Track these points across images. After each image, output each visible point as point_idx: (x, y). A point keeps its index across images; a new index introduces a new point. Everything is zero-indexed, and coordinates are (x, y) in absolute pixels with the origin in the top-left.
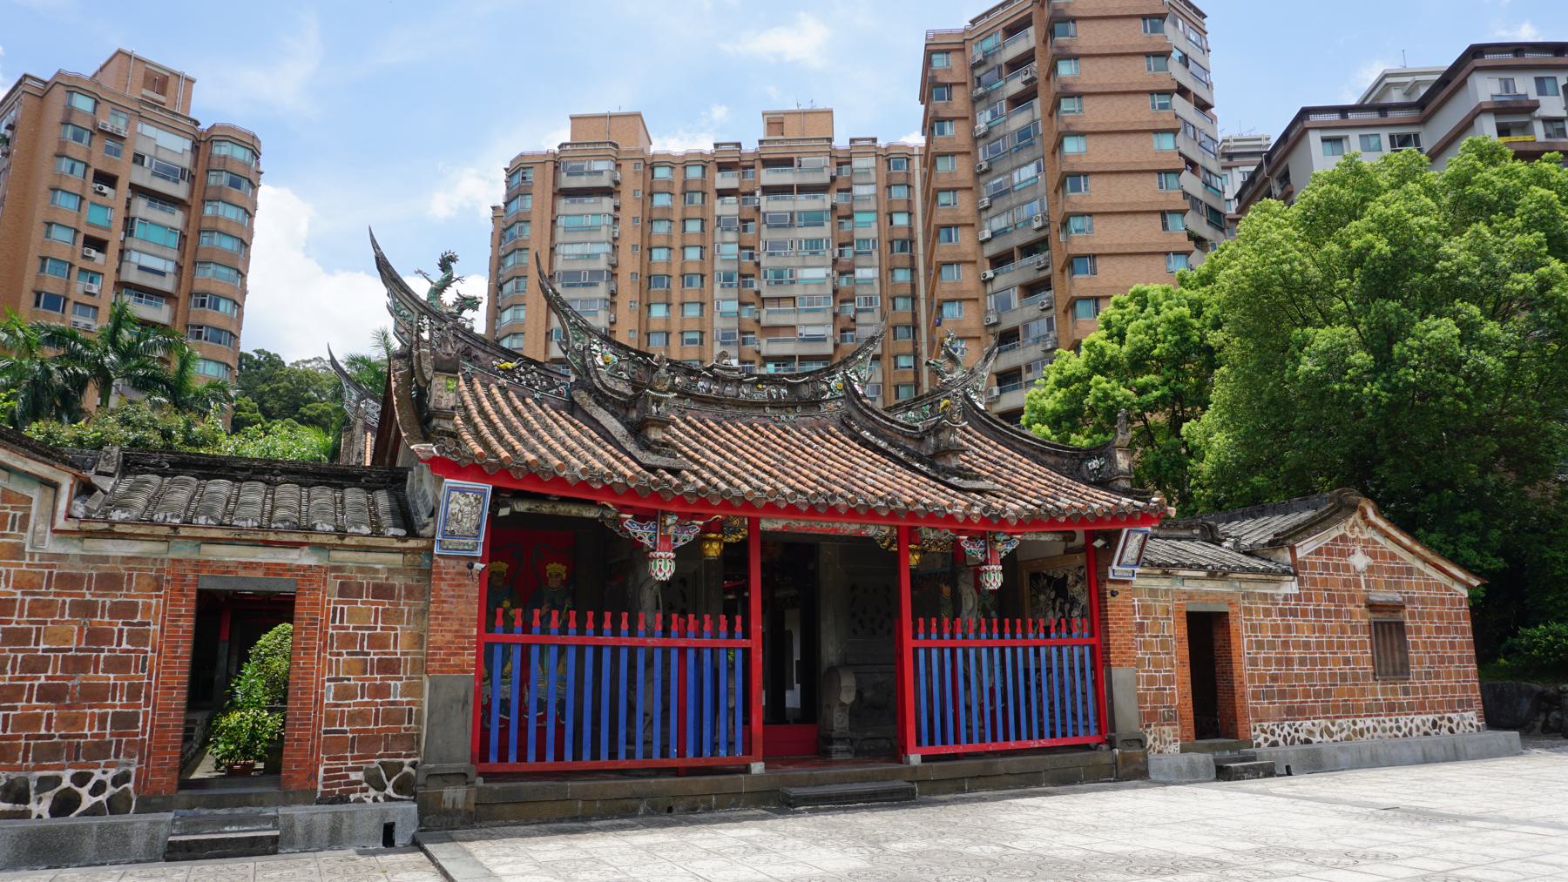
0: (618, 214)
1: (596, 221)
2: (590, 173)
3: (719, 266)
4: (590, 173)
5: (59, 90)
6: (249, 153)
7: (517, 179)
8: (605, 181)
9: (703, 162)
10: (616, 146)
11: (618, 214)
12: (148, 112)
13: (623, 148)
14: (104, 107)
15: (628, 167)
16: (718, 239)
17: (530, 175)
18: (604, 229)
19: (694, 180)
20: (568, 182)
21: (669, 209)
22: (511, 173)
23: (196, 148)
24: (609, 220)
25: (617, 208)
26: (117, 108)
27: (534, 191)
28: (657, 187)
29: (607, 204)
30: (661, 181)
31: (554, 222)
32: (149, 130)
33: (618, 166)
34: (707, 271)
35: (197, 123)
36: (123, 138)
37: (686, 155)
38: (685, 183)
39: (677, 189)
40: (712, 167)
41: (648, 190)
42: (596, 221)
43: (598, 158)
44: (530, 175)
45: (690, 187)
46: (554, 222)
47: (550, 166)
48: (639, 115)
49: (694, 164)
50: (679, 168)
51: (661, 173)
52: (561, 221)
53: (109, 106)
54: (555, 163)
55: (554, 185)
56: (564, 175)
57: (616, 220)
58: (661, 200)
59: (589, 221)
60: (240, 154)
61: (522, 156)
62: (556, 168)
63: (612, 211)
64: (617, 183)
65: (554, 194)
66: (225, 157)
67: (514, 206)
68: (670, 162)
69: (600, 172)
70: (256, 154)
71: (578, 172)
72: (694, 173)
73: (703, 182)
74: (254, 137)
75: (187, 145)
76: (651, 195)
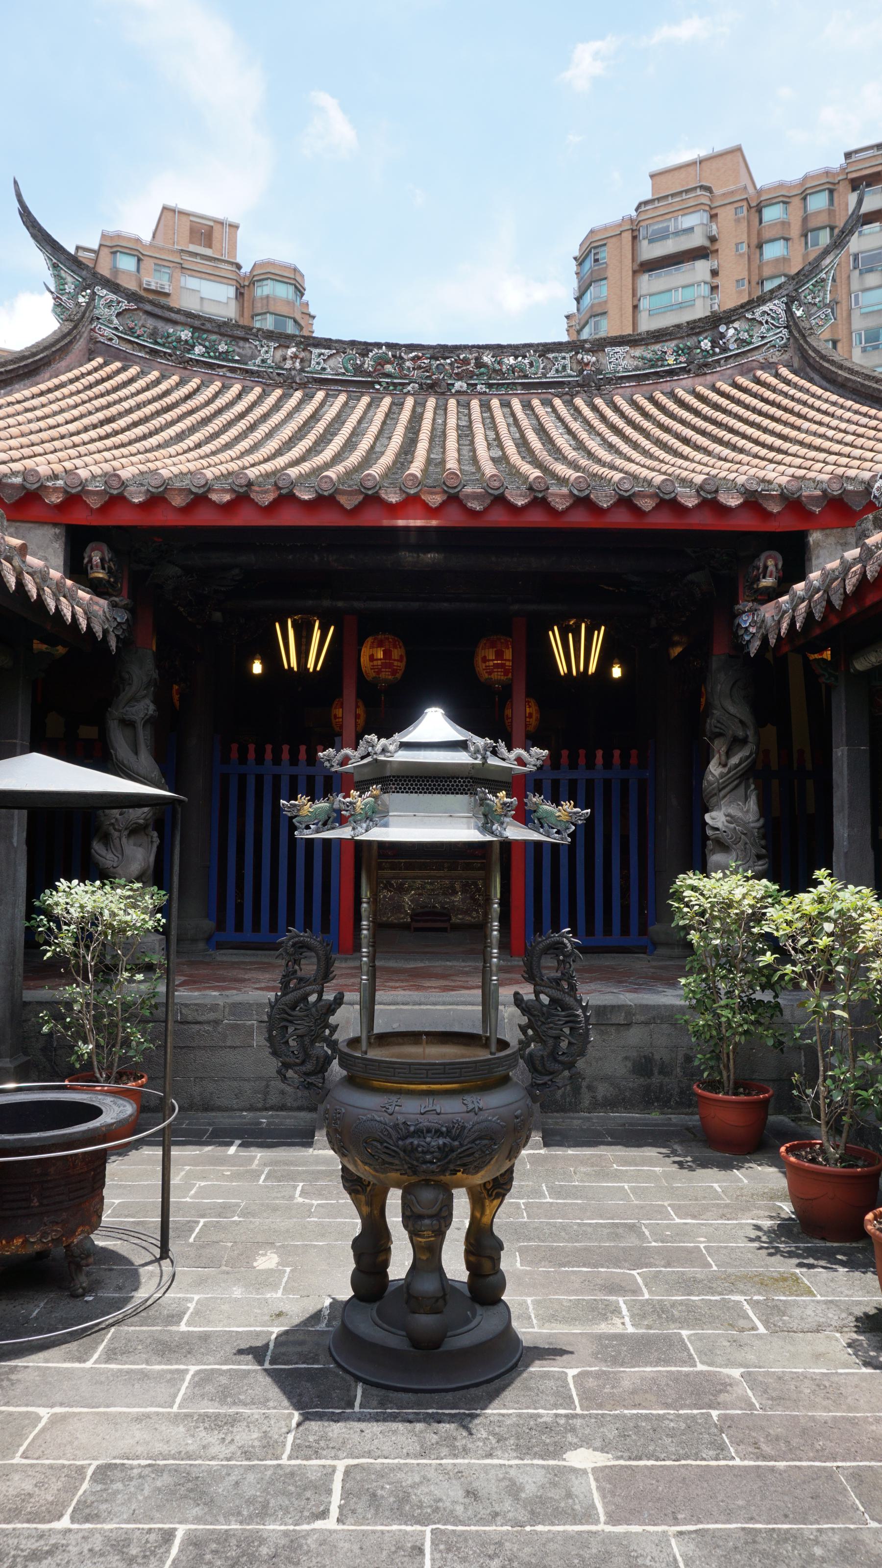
0: (716, 281)
1: (689, 294)
2: (677, 233)
3: (858, 323)
4: (677, 233)
5: (105, 252)
6: (291, 289)
7: (588, 265)
8: (697, 240)
9: (830, 185)
10: (708, 189)
11: (716, 281)
12: (190, 262)
13: (717, 191)
14: (148, 264)
15: (726, 215)
16: (855, 285)
17: (603, 255)
18: (699, 303)
19: (818, 213)
20: (650, 251)
21: (785, 260)
22: (580, 261)
23: (240, 295)
24: (705, 290)
25: (714, 273)
26: (160, 264)
27: (609, 274)
28: (767, 235)
29: (702, 268)
30: (772, 225)
31: (635, 307)
32: (192, 283)
33: (713, 217)
34: (842, 334)
35: (239, 267)
36: (167, 295)
37: (806, 178)
38: (805, 220)
39: (795, 231)
40: (844, 187)
41: (754, 242)
42: (689, 294)
43: (687, 211)
44: (603, 255)
45: (812, 224)
46: (635, 307)
47: (627, 236)
48: (738, 150)
49: (817, 190)
50: (796, 202)
51: (772, 214)
52: (644, 304)
53: (152, 261)
54: (634, 230)
55: (633, 260)
56: (645, 243)
57: (714, 289)
58: (773, 251)
59: (679, 296)
60: (284, 292)
61: (592, 232)
62: (634, 238)
63: (708, 277)
64: (713, 239)
65: (635, 272)
66: (268, 297)
67: (587, 299)
68: (782, 196)
69: (691, 229)
70: (300, 291)
71: (664, 235)
72: (818, 202)
73: (831, 212)
74: (295, 270)
75: (231, 292)
76: (760, 247)
